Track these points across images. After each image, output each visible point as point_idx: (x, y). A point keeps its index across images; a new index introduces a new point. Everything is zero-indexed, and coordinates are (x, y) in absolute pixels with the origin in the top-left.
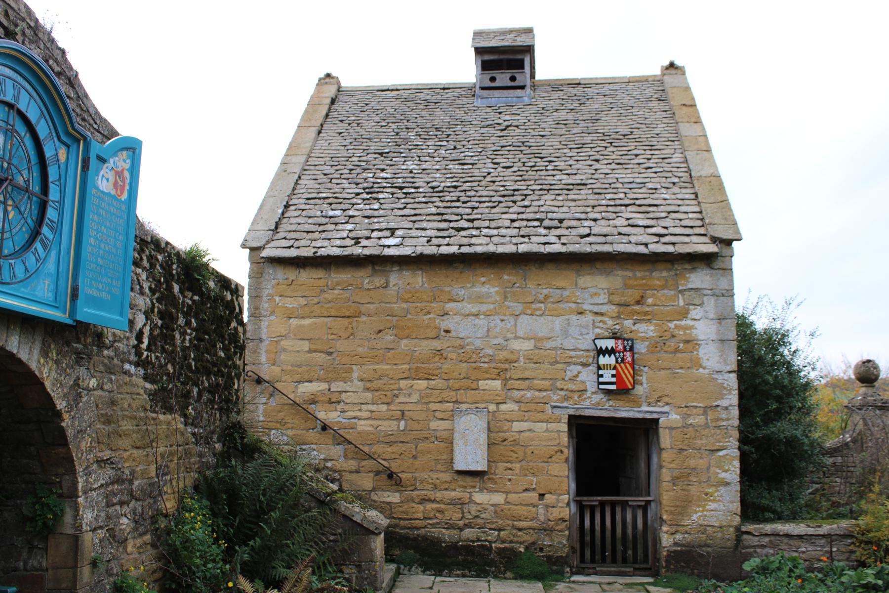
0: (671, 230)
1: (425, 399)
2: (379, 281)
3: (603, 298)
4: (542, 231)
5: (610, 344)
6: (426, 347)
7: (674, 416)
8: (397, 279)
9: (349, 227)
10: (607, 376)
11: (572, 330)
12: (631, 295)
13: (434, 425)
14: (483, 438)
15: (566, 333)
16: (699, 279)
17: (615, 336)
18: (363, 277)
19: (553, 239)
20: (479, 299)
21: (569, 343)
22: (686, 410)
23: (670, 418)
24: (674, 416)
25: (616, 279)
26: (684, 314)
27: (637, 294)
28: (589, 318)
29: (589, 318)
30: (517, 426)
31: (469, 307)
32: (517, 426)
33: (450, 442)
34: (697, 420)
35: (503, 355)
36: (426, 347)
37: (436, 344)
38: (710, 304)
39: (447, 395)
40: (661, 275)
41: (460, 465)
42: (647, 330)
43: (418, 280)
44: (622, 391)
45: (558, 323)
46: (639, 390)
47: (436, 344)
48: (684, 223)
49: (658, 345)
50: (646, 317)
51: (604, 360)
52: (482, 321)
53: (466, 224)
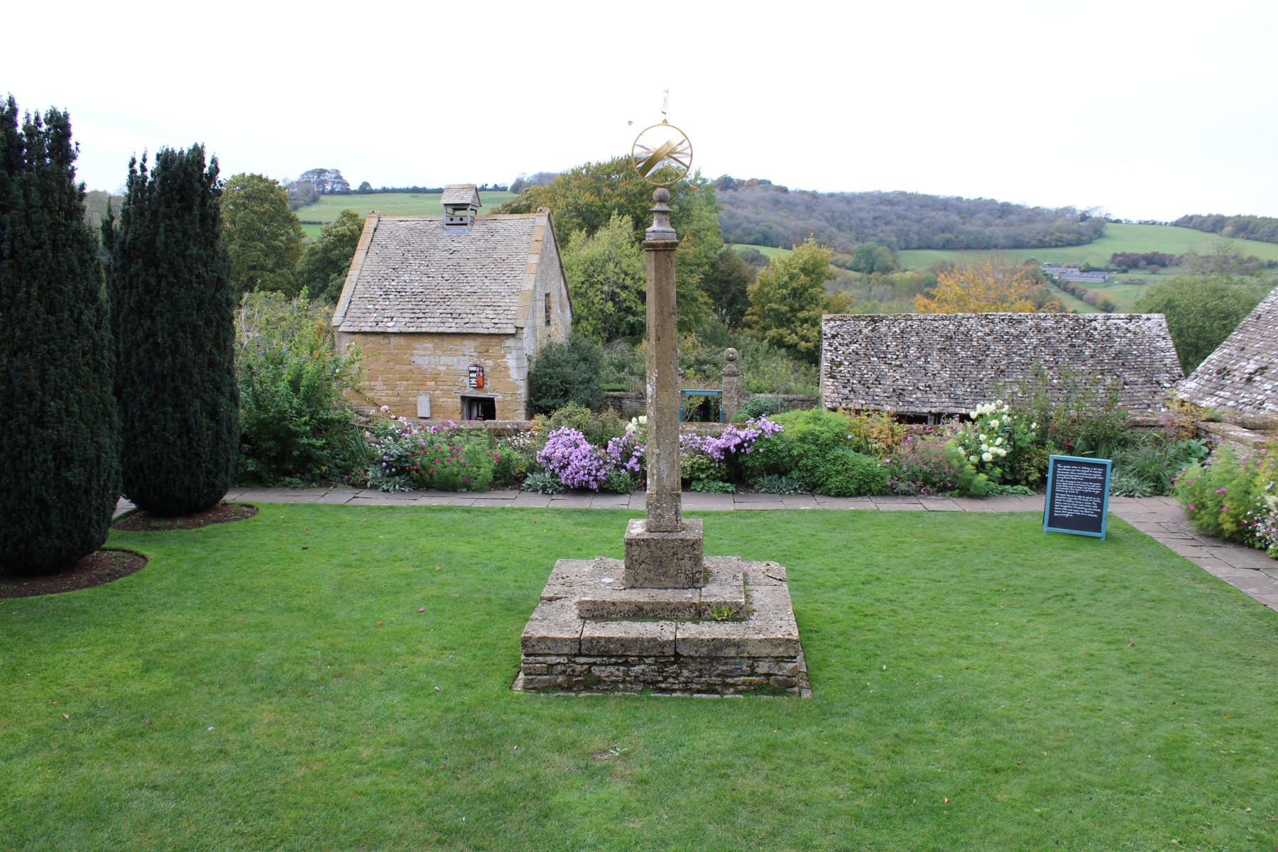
0: (503, 321)
1: (406, 389)
2: (387, 341)
3: (472, 350)
4: (451, 320)
5: (474, 369)
6: (405, 368)
7: (500, 397)
8: (393, 340)
9: (375, 315)
10: (473, 381)
11: (462, 362)
12: (484, 348)
13: (410, 399)
14: (428, 405)
15: (459, 364)
16: (510, 343)
17: (476, 366)
18: (379, 339)
19: (453, 325)
20: (425, 349)
21: (460, 368)
22: (505, 395)
23: (498, 398)
24: (500, 397)
25: (479, 341)
26: (504, 357)
27: (485, 348)
28: (467, 357)
29: (467, 357)
30: (441, 400)
31: (422, 352)
32: (441, 400)
33: (416, 405)
34: (509, 399)
35: (435, 372)
36: (405, 368)
37: (410, 367)
38: (514, 352)
39: (414, 387)
40: (495, 340)
41: (420, 415)
42: (489, 363)
43: (402, 341)
44: (479, 386)
45: (455, 359)
46: (486, 386)
47: (410, 367)
48: (509, 317)
49: (493, 369)
50: (490, 358)
51: (472, 375)
52: (427, 358)
53: (421, 315)
